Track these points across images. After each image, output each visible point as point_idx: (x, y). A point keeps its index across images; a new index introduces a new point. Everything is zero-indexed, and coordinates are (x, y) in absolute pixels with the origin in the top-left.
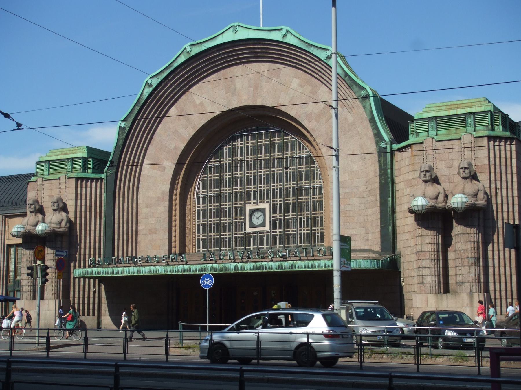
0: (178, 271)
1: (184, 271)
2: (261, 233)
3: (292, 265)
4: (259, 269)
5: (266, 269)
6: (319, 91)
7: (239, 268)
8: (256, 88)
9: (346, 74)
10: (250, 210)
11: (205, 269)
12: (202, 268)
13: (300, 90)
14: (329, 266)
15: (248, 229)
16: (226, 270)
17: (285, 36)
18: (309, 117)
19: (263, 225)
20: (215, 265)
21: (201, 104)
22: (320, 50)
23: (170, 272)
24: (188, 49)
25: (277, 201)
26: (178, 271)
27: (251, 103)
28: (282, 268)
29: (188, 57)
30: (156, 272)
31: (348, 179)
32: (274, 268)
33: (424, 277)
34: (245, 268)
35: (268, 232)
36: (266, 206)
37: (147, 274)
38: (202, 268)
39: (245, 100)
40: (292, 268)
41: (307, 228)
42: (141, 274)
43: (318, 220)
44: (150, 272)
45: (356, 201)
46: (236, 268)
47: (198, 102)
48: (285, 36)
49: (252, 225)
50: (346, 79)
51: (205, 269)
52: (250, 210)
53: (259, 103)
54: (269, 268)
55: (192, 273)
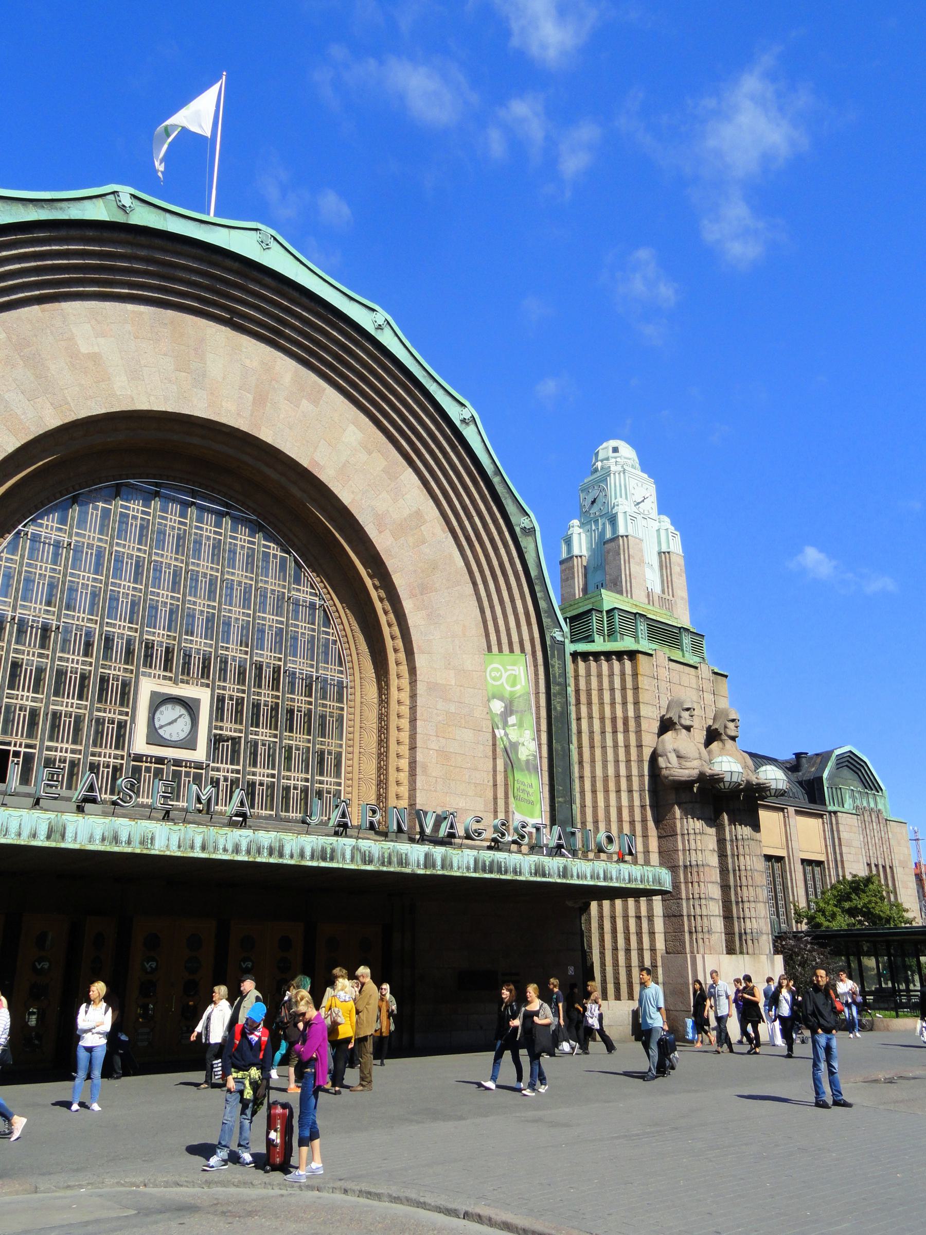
0: (237, 850)
1: (259, 852)
2: (177, 762)
3: (565, 868)
4: (491, 872)
5: (506, 872)
6: (402, 477)
7: (439, 863)
8: (261, 400)
9: (498, 472)
10: (154, 694)
11: (333, 851)
12: (323, 850)
13: (363, 456)
14: (636, 880)
15: (140, 744)
16: (400, 863)
17: (379, 327)
18: (380, 520)
19: (189, 743)
20: (364, 844)
21: (95, 358)
22: (448, 399)
23: (203, 848)
24: (126, 201)
25: (231, 689)
26: (237, 850)
27: (242, 424)
28: (544, 875)
29: (120, 218)
30: (142, 843)
31: (453, 682)
32: (526, 870)
33: (712, 918)
34: (455, 865)
35: (199, 766)
36: (203, 695)
37: (97, 846)
38: (323, 850)
39: (231, 411)
40: (565, 876)
41: (304, 776)
42: (68, 844)
43: (329, 760)
44: (116, 839)
45: (467, 735)
46: (429, 861)
47: (84, 350)
48: (379, 327)
49: (154, 738)
50: (496, 480)
51: (333, 851)
52: (154, 694)
53: (267, 435)
54: (515, 872)
55: (287, 861)
